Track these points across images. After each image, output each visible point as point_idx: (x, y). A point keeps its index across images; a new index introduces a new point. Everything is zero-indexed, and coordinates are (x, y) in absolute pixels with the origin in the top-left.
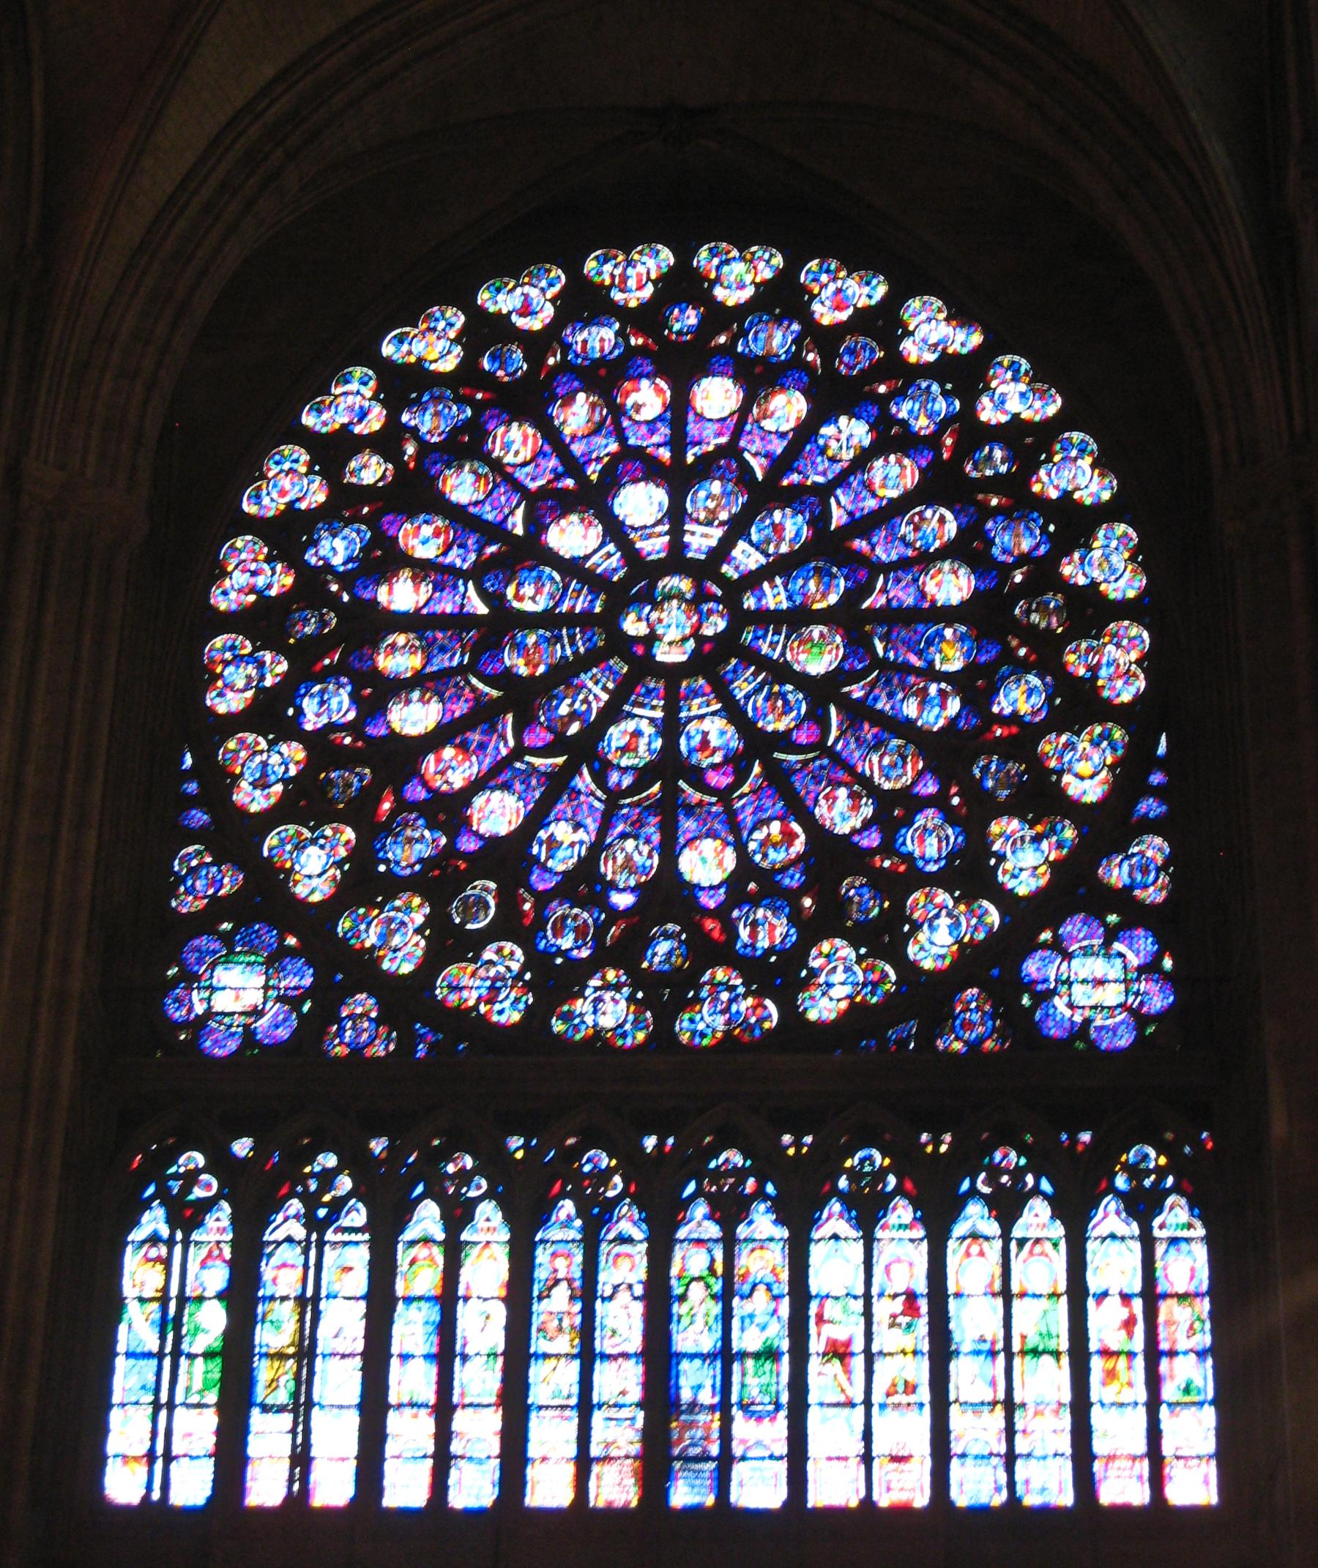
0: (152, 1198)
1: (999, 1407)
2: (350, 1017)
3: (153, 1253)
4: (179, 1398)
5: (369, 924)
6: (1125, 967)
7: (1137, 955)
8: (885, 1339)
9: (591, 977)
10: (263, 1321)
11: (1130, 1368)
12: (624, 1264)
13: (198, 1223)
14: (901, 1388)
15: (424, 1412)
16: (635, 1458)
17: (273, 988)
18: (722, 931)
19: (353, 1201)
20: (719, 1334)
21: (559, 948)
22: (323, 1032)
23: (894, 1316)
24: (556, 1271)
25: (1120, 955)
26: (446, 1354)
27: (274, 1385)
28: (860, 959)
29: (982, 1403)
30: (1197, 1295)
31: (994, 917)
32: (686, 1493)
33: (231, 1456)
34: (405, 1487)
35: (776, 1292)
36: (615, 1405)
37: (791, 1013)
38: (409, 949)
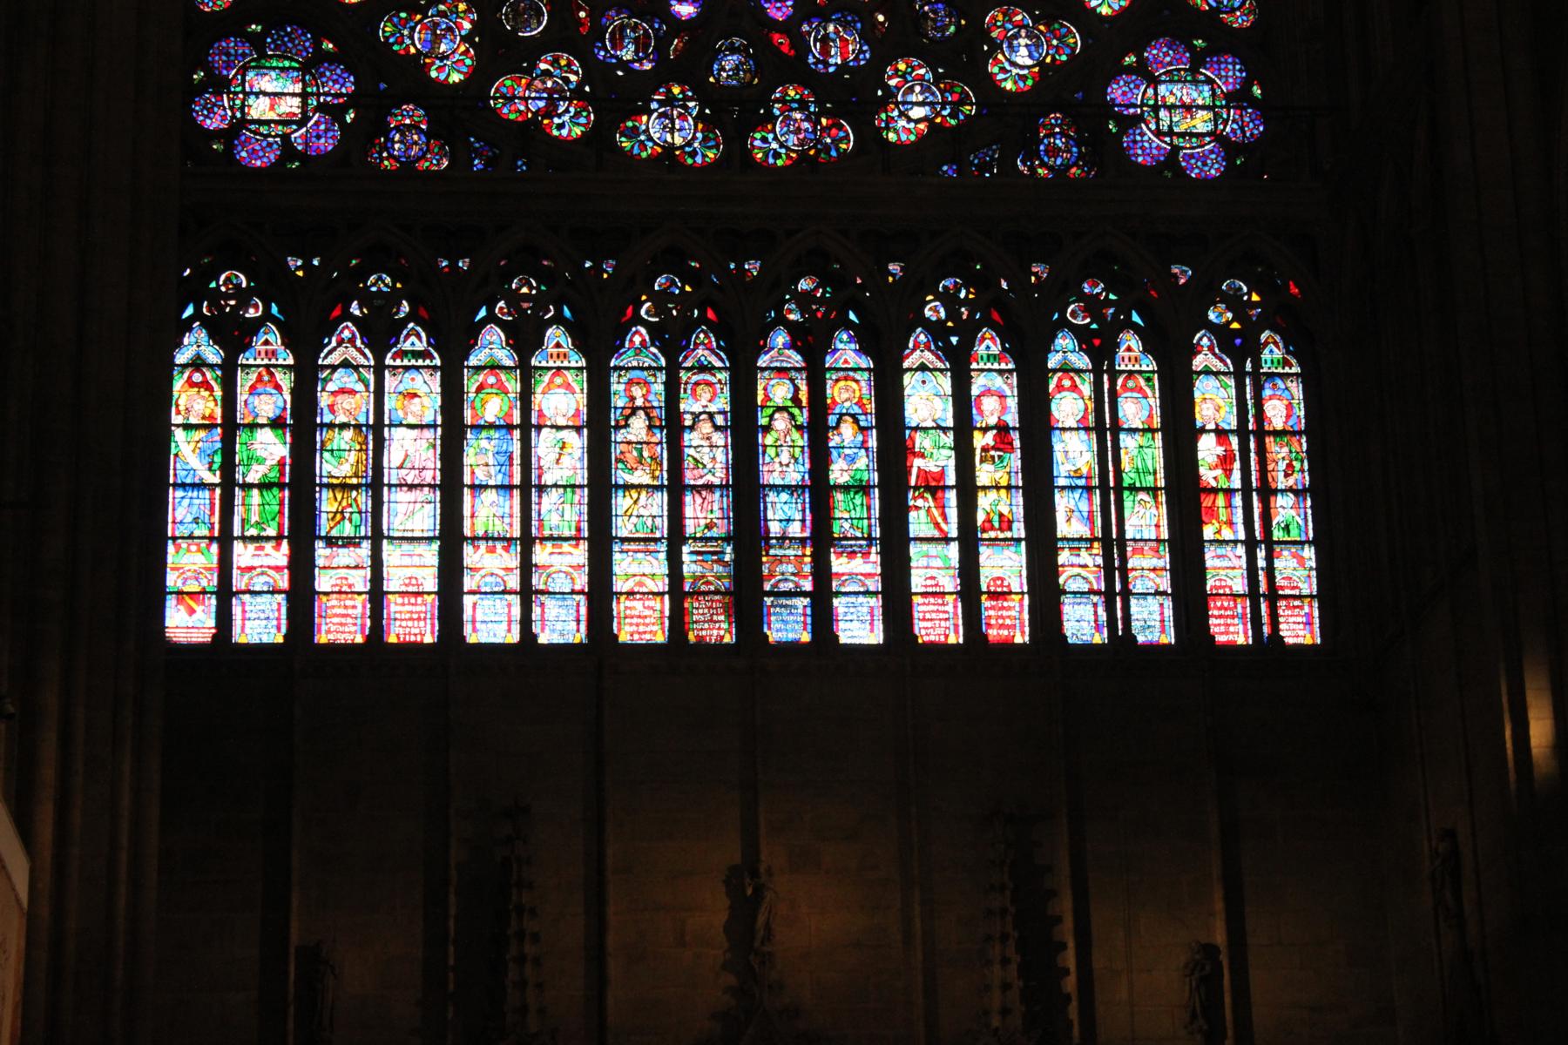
0: (192, 319)
1: (1096, 544)
2: (397, 128)
3: (197, 377)
4: (237, 532)
5: (413, 29)
6: (1214, 95)
7: (1226, 83)
8: (984, 474)
9: (656, 92)
10: (322, 450)
11: (1229, 506)
12: (705, 394)
13: (248, 346)
14: (996, 525)
15: (499, 545)
16: (726, 593)
17: (312, 94)
18: (792, 46)
19: (411, 325)
20: (807, 466)
21: (620, 59)
22: (370, 140)
23: (985, 449)
24: (633, 399)
25: (1209, 81)
26: (528, 488)
27: (338, 517)
28: (938, 79)
29: (1080, 539)
30: (1293, 433)
31: (1076, 40)
32: (787, 626)
33: (301, 598)
34: (490, 622)
35: (863, 424)
36: (701, 539)
37: (870, 138)
38: (457, 57)
